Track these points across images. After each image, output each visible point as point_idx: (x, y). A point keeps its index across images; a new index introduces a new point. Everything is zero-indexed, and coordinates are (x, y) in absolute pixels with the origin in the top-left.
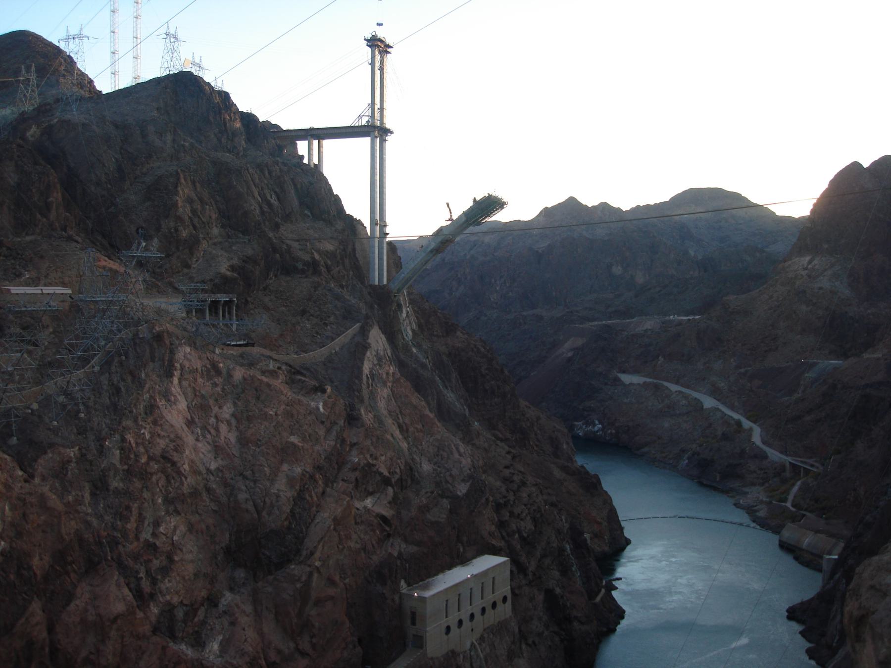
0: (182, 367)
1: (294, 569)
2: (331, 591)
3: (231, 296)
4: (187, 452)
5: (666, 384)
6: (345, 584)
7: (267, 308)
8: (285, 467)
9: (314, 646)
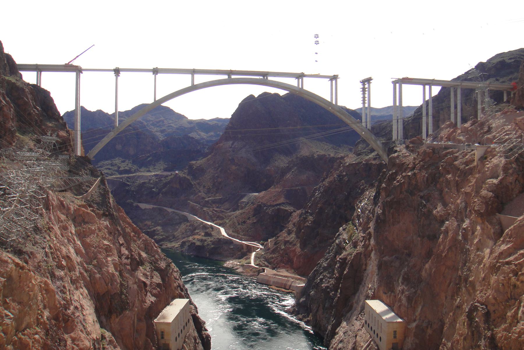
8: (109, 259)
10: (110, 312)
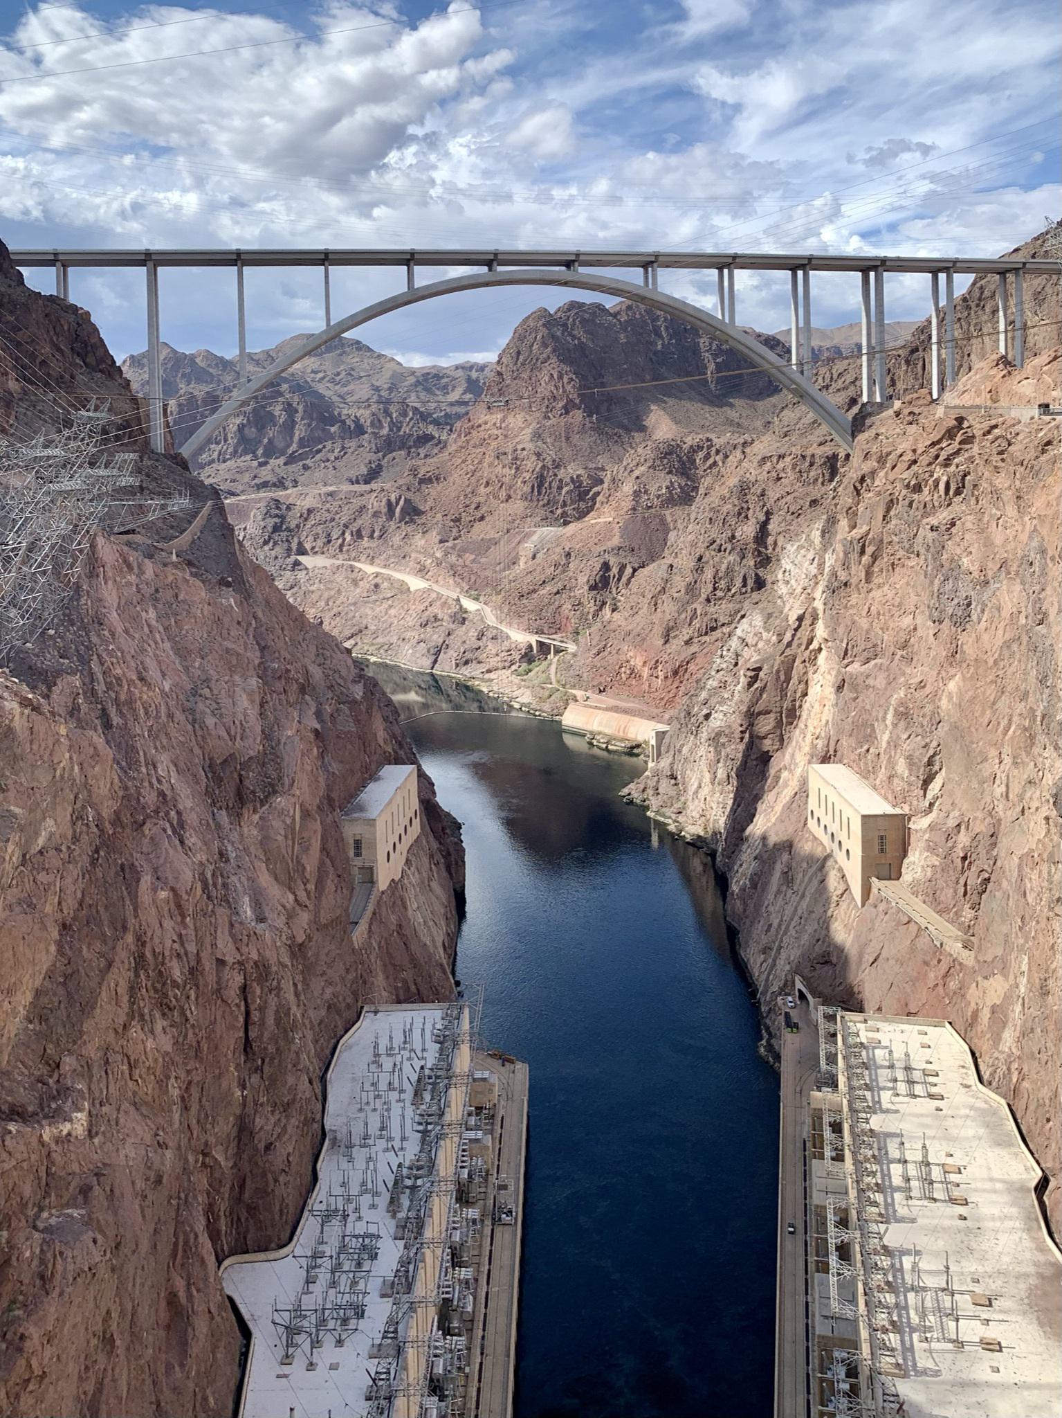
1: (280, 801)
5: (357, 564)
10: (241, 798)
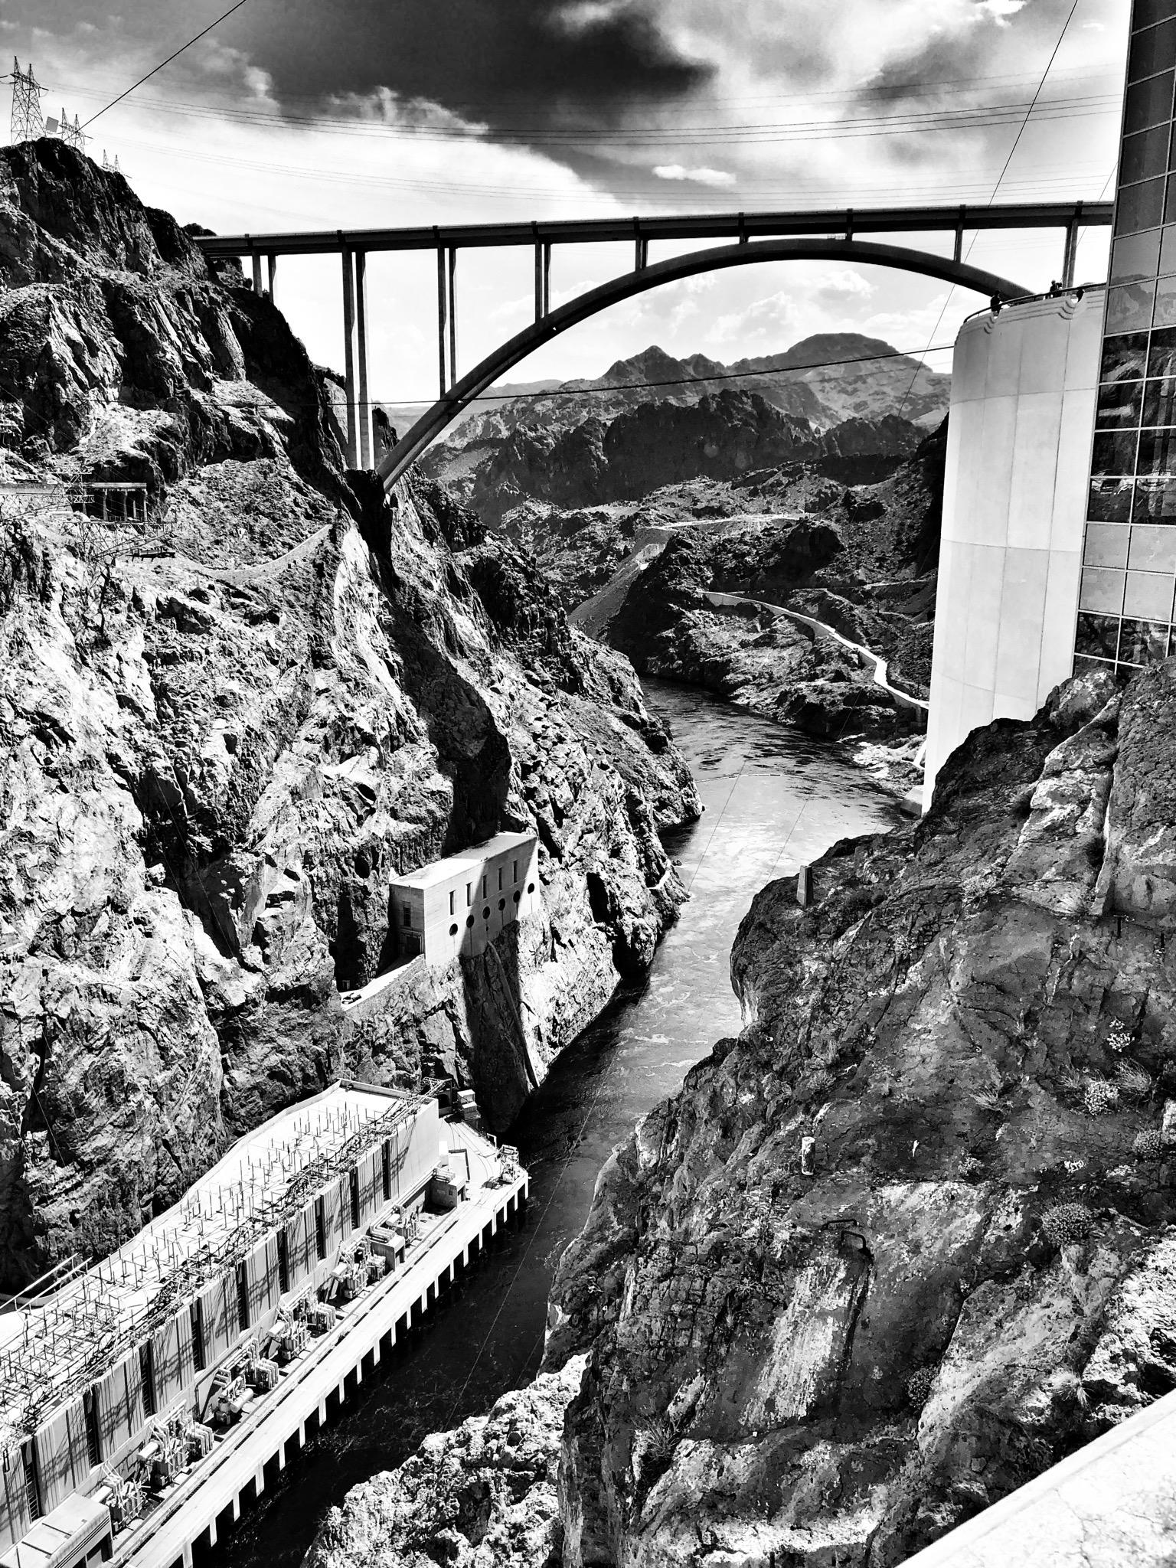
0: (64, 587)
2: (289, 885)
3: (138, 485)
4: (76, 706)
6: (310, 876)
7: (194, 502)
8: (220, 723)
9: (266, 959)
